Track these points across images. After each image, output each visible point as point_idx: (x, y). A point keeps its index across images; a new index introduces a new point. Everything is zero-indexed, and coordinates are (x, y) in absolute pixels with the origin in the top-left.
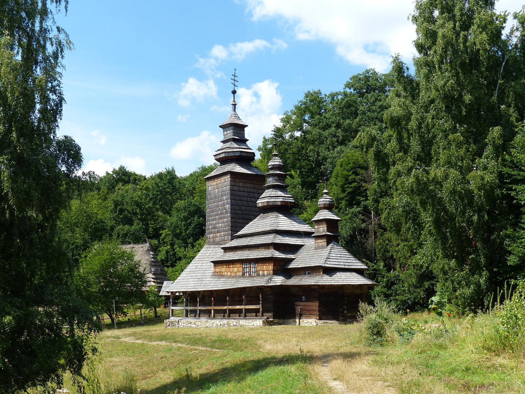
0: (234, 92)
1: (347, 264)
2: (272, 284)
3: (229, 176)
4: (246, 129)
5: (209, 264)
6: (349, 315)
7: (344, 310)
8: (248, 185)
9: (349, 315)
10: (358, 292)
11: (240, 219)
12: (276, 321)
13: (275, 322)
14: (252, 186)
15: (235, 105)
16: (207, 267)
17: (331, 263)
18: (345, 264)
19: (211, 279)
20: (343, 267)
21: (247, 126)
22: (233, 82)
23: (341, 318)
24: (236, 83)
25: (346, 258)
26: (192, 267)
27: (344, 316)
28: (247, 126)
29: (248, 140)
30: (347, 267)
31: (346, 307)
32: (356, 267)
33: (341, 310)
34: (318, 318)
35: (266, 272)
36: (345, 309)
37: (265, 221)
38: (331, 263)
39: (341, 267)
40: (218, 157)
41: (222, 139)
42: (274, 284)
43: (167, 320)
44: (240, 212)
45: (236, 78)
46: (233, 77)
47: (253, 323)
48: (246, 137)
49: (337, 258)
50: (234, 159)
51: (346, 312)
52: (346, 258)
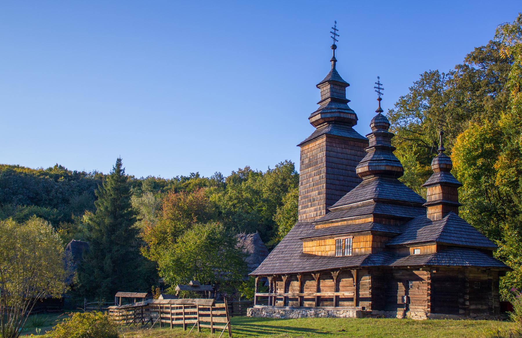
0: (334, 47)
1: (470, 240)
2: (369, 265)
3: (325, 139)
4: (347, 88)
5: (299, 243)
6: (472, 307)
7: (465, 300)
8: (349, 151)
9: (472, 307)
10: (485, 277)
11: (337, 190)
12: (375, 312)
13: (372, 313)
14: (353, 152)
15: (334, 60)
16: (296, 246)
17: (448, 238)
18: (467, 240)
19: (299, 260)
20: (465, 244)
21: (348, 85)
22: (333, 36)
23: (461, 311)
24: (337, 38)
25: (468, 233)
26: (280, 248)
27: (465, 309)
28: (348, 85)
29: (350, 101)
30: (468, 244)
31: (467, 297)
32: (481, 245)
33: (461, 300)
34: (429, 309)
35: (363, 250)
36: (467, 300)
37: (365, 189)
38: (448, 238)
39: (461, 243)
40: (314, 119)
41: (320, 100)
42: (373, 265)
43: (250, 309)
44: (337, 182)
45: (337, 32)
46: (333, 31)
47: (344, 314)
48: (348, 97)
49: (456, 232)
50: (332, 121)
51: (468, 303)
52: (468, 233)
